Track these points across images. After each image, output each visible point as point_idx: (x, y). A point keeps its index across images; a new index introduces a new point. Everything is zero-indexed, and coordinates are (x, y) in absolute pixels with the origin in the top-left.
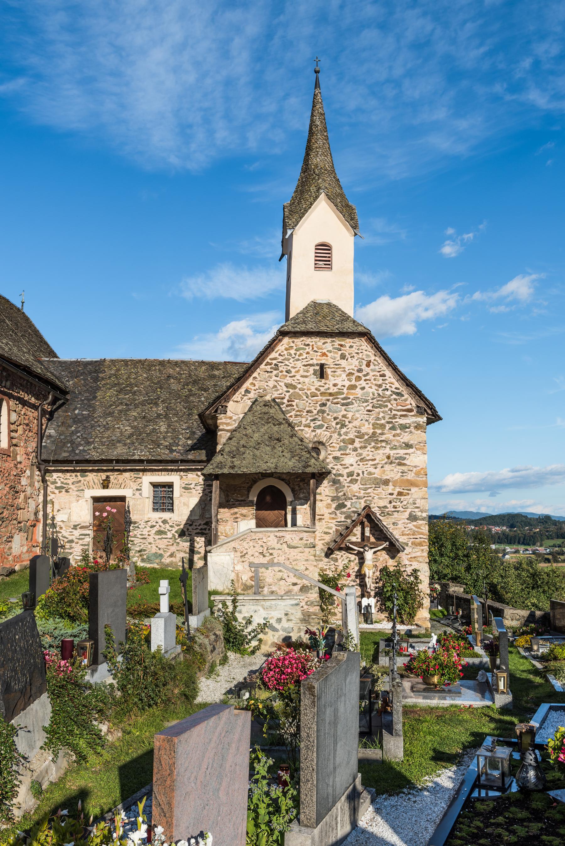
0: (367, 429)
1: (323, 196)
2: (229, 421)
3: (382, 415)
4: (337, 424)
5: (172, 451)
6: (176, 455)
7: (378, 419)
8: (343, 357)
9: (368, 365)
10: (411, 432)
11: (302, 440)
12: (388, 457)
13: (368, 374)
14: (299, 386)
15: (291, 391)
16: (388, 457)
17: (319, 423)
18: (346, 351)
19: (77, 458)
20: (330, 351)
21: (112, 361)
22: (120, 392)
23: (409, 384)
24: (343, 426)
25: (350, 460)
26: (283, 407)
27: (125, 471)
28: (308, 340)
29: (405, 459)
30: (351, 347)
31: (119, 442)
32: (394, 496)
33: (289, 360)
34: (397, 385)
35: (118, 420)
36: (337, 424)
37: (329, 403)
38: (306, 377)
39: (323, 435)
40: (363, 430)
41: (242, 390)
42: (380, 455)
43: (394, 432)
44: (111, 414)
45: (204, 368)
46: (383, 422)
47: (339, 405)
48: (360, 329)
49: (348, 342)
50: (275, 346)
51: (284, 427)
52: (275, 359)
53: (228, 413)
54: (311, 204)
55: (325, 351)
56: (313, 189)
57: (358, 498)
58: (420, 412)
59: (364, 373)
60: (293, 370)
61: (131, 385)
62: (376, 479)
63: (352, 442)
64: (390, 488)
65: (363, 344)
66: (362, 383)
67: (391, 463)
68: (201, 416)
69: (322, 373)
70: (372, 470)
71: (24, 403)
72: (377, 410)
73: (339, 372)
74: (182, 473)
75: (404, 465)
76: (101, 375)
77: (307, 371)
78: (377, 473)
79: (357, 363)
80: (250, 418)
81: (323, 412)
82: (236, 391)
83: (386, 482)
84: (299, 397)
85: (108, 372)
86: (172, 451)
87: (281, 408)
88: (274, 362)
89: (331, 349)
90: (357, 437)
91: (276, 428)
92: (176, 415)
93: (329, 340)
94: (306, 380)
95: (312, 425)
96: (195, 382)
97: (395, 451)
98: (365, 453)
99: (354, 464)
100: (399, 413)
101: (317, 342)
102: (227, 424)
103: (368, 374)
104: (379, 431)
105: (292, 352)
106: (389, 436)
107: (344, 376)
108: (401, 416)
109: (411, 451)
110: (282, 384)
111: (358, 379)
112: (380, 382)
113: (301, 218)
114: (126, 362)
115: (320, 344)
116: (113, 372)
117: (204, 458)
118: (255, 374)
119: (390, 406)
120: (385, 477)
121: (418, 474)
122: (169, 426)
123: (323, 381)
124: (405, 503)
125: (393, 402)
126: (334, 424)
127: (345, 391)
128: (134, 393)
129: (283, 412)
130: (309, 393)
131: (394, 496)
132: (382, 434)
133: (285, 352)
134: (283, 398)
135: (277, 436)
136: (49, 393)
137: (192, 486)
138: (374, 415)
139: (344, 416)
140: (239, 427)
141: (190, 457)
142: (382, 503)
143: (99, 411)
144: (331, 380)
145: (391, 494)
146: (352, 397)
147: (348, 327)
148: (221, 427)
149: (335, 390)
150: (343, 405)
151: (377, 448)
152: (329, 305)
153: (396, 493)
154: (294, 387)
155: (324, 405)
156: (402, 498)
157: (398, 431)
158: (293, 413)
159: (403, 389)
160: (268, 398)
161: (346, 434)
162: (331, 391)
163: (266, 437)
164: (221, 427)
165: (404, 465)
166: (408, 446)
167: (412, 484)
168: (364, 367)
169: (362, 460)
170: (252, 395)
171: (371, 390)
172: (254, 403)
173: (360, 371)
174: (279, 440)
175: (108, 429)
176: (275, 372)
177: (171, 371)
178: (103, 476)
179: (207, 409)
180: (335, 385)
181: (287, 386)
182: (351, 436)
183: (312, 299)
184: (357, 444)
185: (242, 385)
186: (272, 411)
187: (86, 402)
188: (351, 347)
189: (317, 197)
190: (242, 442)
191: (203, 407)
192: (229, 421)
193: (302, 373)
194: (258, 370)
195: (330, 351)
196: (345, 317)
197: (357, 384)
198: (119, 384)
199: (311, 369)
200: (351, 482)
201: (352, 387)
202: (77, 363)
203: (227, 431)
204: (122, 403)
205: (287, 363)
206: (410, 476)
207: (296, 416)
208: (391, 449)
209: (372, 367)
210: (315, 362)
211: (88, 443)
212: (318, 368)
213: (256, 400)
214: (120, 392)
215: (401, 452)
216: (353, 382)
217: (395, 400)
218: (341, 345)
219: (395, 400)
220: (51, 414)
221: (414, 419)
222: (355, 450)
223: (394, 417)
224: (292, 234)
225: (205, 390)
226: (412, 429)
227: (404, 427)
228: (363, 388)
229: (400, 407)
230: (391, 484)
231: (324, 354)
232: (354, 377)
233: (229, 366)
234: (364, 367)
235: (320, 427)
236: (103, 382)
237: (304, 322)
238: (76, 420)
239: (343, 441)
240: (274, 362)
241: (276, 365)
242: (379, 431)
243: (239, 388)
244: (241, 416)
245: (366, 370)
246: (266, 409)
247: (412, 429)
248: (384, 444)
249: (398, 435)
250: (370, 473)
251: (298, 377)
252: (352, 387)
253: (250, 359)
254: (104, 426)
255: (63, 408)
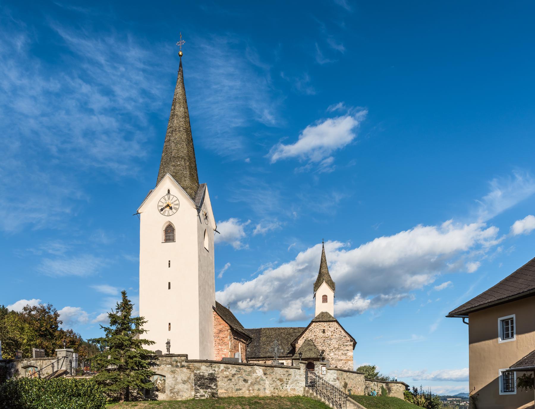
0: (336, 346)
1: (324, 282)
2: (299, 345)
3: (340, 342)
4: (328, 345)
5: (283, 354)
6: (284, 355)
7: (339, 343)
8: (330, 327)
9: (337, 329)
10: (348, 347)
11: (318, 349)
12: (342, 353)
13: (336, 332)
14: (318, 335)
15: (316, 337)
16: (342, 353)
17: (323, 345)
18: (331, 325)
19: (257, 357)
20: (326, 326)
21: (264, 328)
22: (267, 338)
23: (348, 334)
24: (330, 346)
25: (332, 354)
26: (313, 341)
27: (270, 360)
28: (320, 323)
29: (347, 354)
30: (332, 324)
31: (268, 352)
32: (344, 364)
33: (315, 329)
34: (345, 334)
35: (267, 346)
36: (328, 345)
37: (326, 340)
38: (320, 333)
39: (324, 348)
40: (335, 346)
41: (302, 337)
42: (340, 353)
43: (344, 347)
44: (265, 344)
45: (292, 330)
46: (341, 344)
47: (329, 340)
48: (334, 320)
49: (331, 323)
50: (311, 325)
51: (313, 346)
52: (311, 328)
53: (299, 343)
54: (321, 284)
55: (325, 326)
56: (322, 279)
57: (334, 364)
58: (351, 341)
59: (336, 331)
60: (316, 331)
61: (270, 336)
62: (339, 359)
63: (332, 350)
64: (343, 361)
65: (335, 324)
66: (335, 334)
67: (343, 355)
68: (291, 344)
69: (324, 332)
70: (338, 357)
71: (243, 342)
72: (339, 341)
73: (329, 331)
74: (286, 360)
75: (347, 355)
76: (261, 333)
77: (320, 331)
78: (339, 358)
79: (334, 329)
80: (304, 344)
81: (324, 342)
82: (301, 337)
83: (342, 360)
84: (318, 338)
85: (263, 332)
86: (283, 354)
87: (313, 342)
88: (311, 329)
89: (326, 325)
90: (334, 348)
91: (311, 347)
92: (284, 344)
93: (326, 323)
94: (319, 334)
95: (321, 346)
96: (289, 334)
97: (344, 352)
98: (336, 352)
99: (333, 355)
100: (345, 342)
101: (323, 323)
102: (298, 346)
103: (336, 332)
104: (340, 347)
105: (316, 326)
106: (342, 348)
107: (330, 332)
108: (346, 342)
109: (348, 351)
110: (313, 335)
111: (334, 333)
112: (340, 334)
113: (318, 288)
114: (268, 329)
115: (323, 324)
116: (264, 332)
117: (292, 356)
118: (305, 333)
119: (343, 340)
120: (341, 359)
121: (350, 358)
122: (282, 347)
123: (324, 334)
124: (347, 365)
125: (344, 339)
126: (327, 345)
127: (330, 336)
128: (271, 338)
129: (313, 343)
130: (320, 337)
131: (344, 364)
132: (341, 347)
133: (314, 327)
134: (313, 339)
135: (311, 349)
136: (248, 339)
137: (289, 363)
138: (338, 342)
139: (330, 343)
140: (301, 347)
141: (288, 355)
142: (340, 366)
143: (262, 344)
144: (327, 334)
145: (343, 363)
146: (332, 338)
147: (331, 319)
148: (297, 347)
149: (328, 336)
150: (330, 340)
151: (339, 351)
152: (326, 313)
153: (344, 363)
154: (316, 336)
155: (325, 340)
156: (346, 364)
157: (345, 346)
158: (316, 343)
159: (347, 335)
160: (309, 339)
161: (331, 348)
162: (326, 336)
163: (308, 349)
164: (297, 347)
165: (347, 355)
166: (348, 350)
167: (349, 360)
168: (336, 330)
169: (335, 354)
170: (305, 338)
171: (338, 336)
172: (305, 340)
173: (334, 331)
174: (311, 350)
175: (265, 349)
176: (311, 332)
177: (282, 331)
178: (264, 361)
179: (293, 342)
180: (327, 335)
181: (314, 335)
182: (332, 348)
183: (321, 311)
184: (334, 350)
185: (302, 335)
186: (310, 342)
187: (257, 341)
188: (332, 324)
189: (323, 282)
190: (302, 351)
191: (292, 341)
192: (299, 345)
193: (318, 332)
194: (306, 332)
195: (326, 326)
196: (330, 316)
197: (334, 334)
198: (266, 335)
199: (321, 331)
200: (332, 360)
201: (332, 335)
202: (253, 330)
203: (298, 348)
204: (268, 341)
205: (314, 329)
206: (348, 358)
207: (317, 343)
208: (343, 351)
209: (338, 329)
210: (322, 329)
211: (260, 353)
212: (323, 330)
213: (306, 340)
214: (267, 338)
215: (346, 352)
216: (333, 334)
217: (344, 338)
218: (329, 324)
219: (344, 338)
220: (248, 345)
221: (349, 343)
222: (333, 352)
223: (344, 343)
224: (316, 293)
225: (292, 336)
226: (349, 346)
227: (346, 345)
228: (335, 335)
229: (346, 340)
230: (343, 360)
231: (324, 327)
232: (333, 333)
233: (300, 329)
234: (336, 330)
235: (323, 346)
236: (262, 335)
237: (319, 318)
238: (255, 346)
239: (330, 350)
240: (311, 329)
241: (311, 330)
242: (340, 347)
243: (301, 336)
244: (302, 344)
245: (336, 330)
246: (308, 342)
247: (349, 346)
248: (341, 350)
249: (345, 347)
250: (337, 358)
251: (317, 333)
252: (332, 335)
253: (306, 326)
254: (263, 348)
255: (251, 343)
